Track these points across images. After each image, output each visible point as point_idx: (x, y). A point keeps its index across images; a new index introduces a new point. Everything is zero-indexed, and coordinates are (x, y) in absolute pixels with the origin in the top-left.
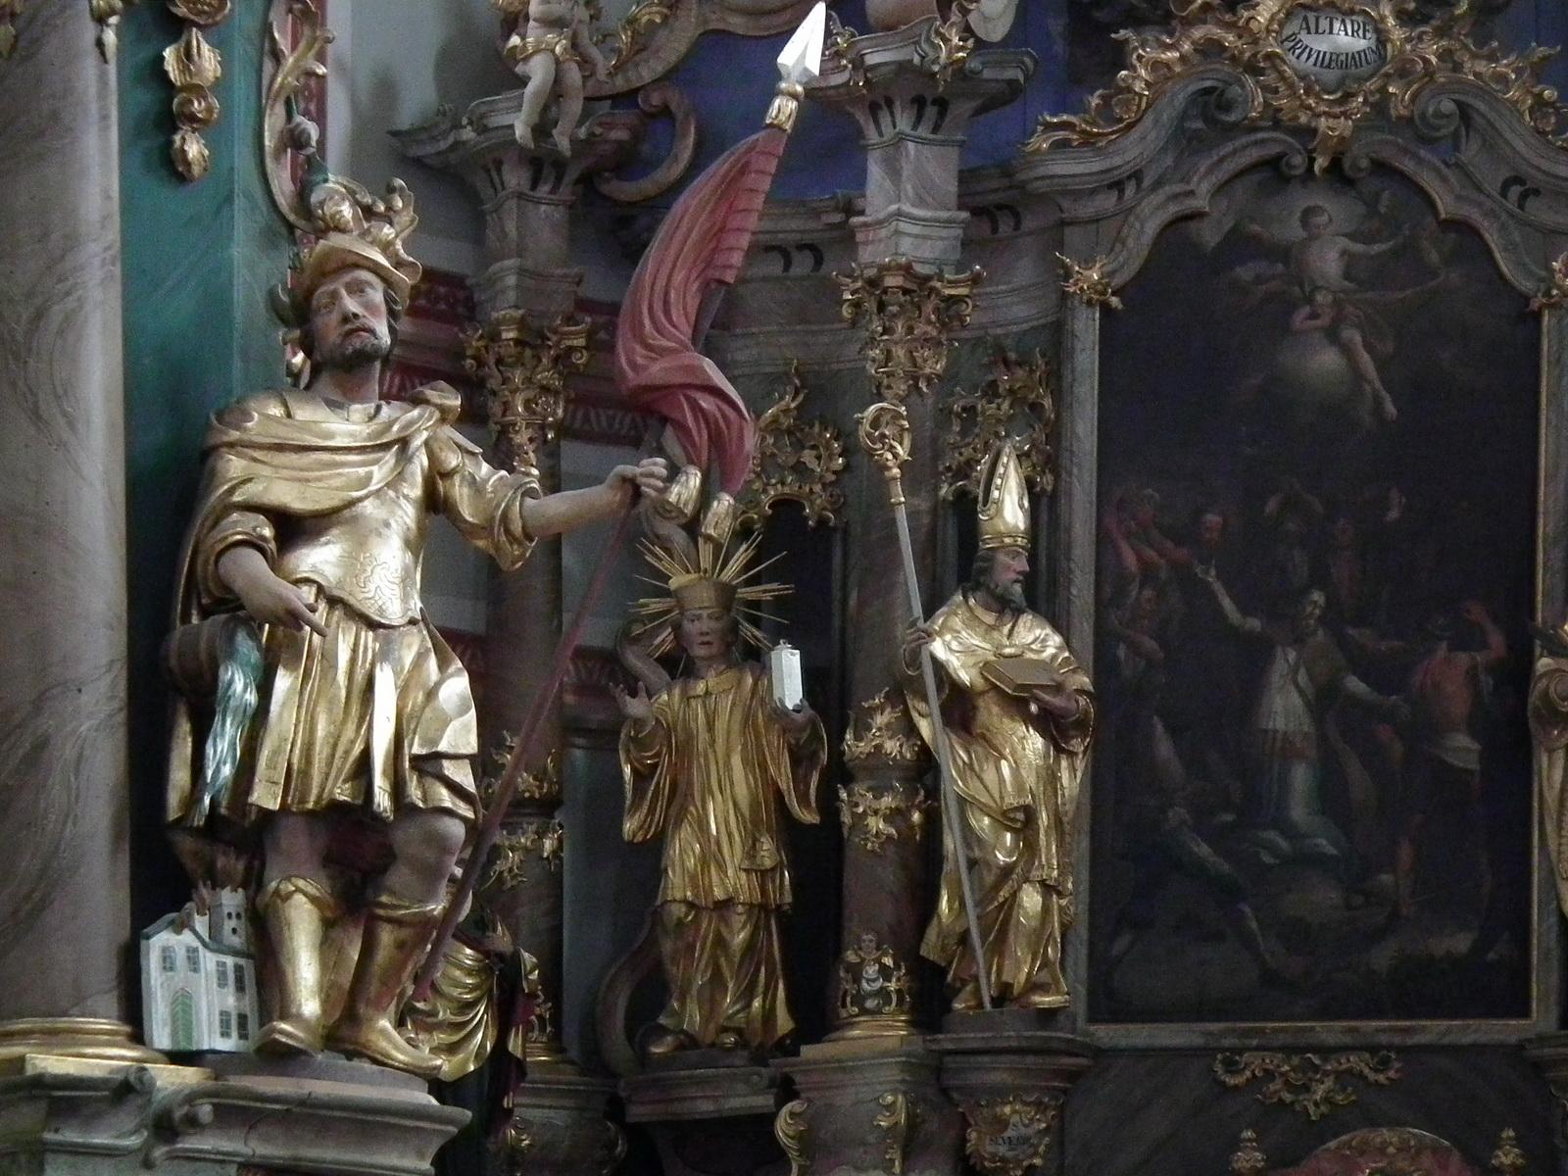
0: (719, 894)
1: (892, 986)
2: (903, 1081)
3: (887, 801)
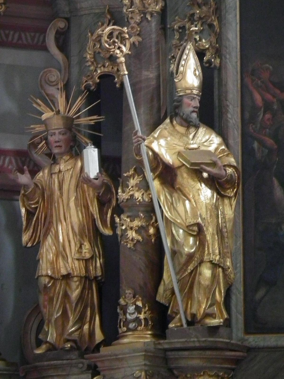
0: (64, 272)
1: (142, 316)
2: (145, 365)
3: (137, 223)
